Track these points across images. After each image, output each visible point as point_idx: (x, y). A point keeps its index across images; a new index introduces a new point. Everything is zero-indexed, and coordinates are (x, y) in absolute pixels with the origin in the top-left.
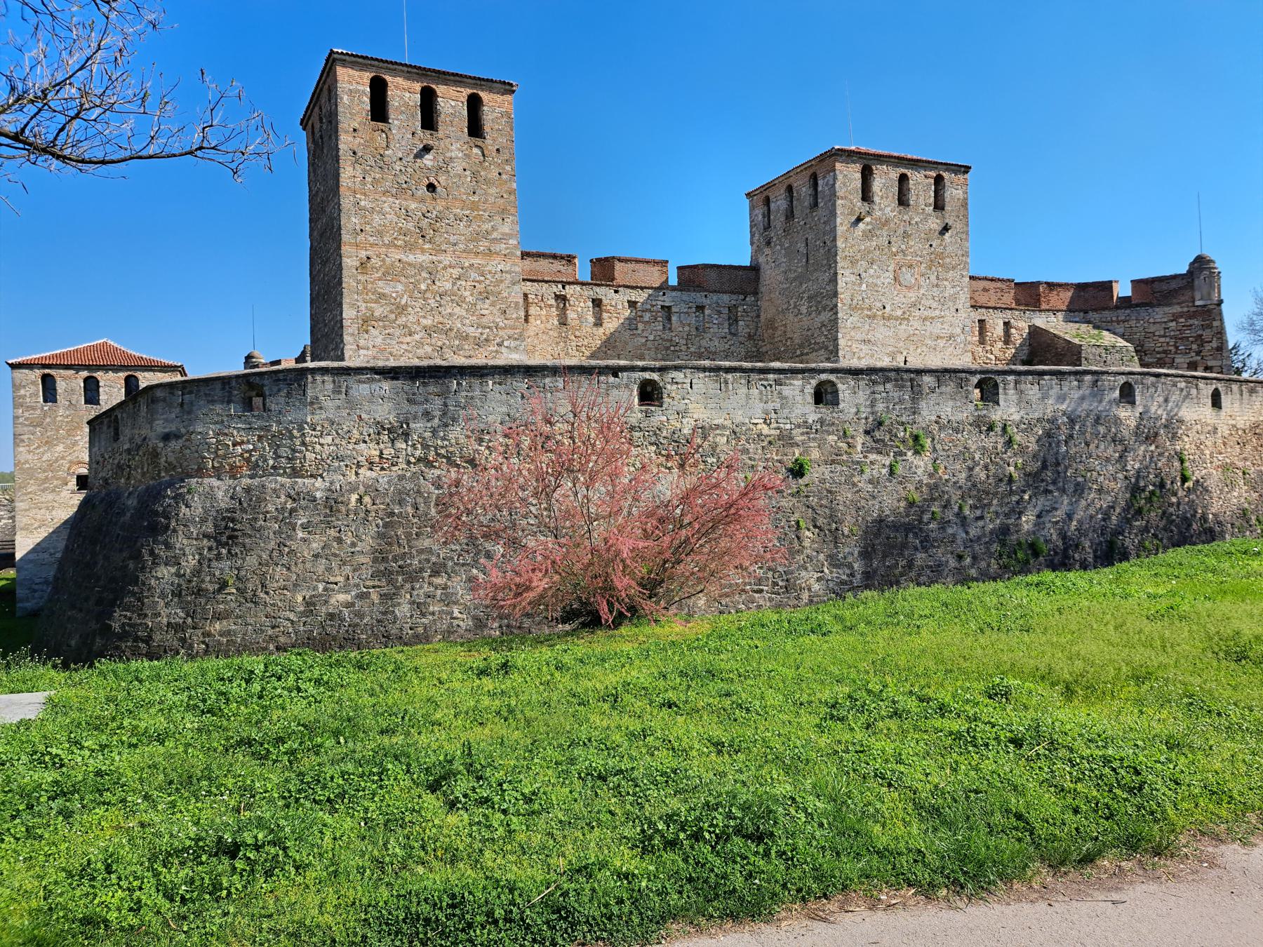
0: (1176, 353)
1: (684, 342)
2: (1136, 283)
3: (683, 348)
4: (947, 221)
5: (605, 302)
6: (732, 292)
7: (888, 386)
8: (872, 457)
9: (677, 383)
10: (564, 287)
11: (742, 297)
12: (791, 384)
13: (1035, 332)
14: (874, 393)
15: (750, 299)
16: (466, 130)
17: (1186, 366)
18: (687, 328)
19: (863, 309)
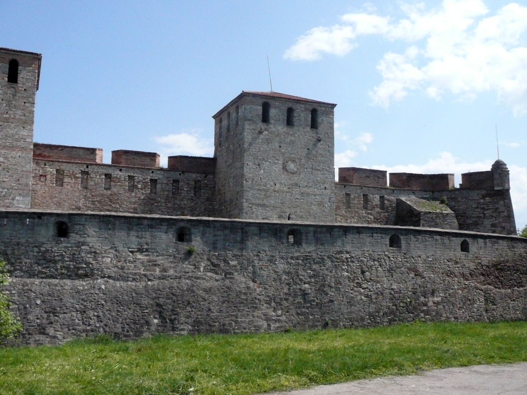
0: (484, 218)
1: (164, 201)
2: (465, 176)
3: (163, 204)
4: (318, 135)
5: (113, 176)
6: (198, 173)
7: (227, 232)
8: (209, 274)
9: (79, 224)
10: (87, 167)
11: (203, 175)
12: (159, 228)
13: (400, 203)
14: (215, 235)
15: (210, 177)
16: (6, 79)
17: (490, 226)
18: (166, 193)
19: (260, 185)
